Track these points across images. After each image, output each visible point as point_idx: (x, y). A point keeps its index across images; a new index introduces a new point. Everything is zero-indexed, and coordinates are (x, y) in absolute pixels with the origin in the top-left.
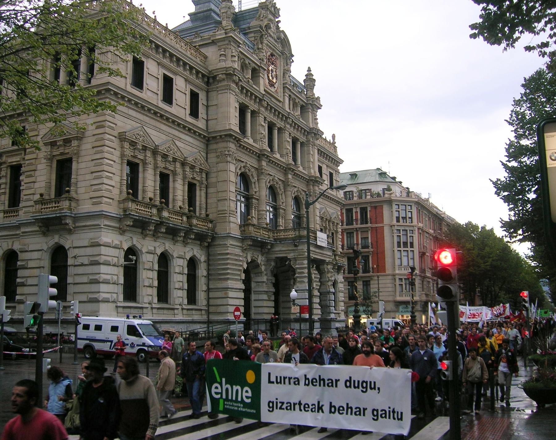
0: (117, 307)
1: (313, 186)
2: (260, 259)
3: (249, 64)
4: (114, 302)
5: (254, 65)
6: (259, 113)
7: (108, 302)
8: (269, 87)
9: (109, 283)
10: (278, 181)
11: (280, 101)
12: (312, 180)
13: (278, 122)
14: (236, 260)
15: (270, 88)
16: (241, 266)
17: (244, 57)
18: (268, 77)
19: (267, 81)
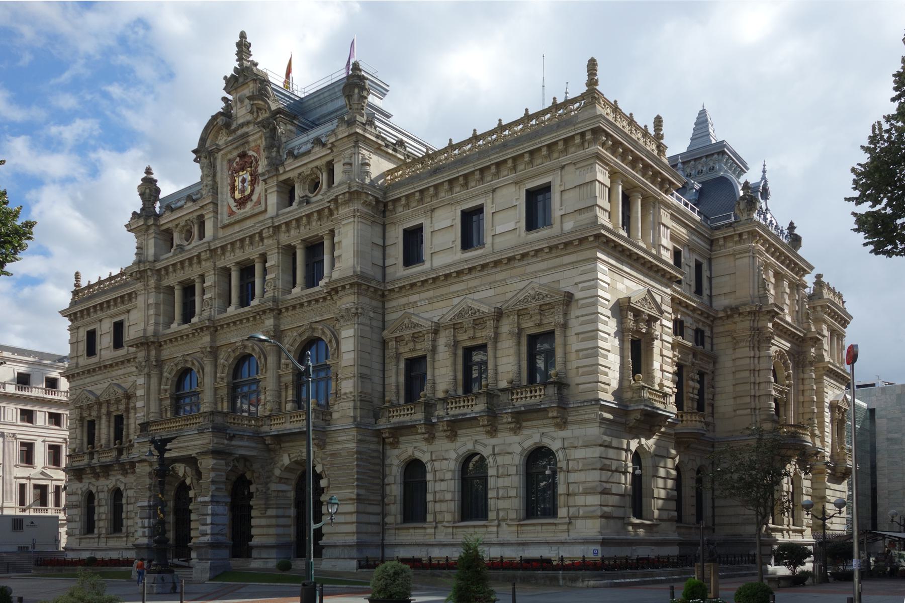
10: (247, 343)
15: (242, 211)
18: (234, 198)
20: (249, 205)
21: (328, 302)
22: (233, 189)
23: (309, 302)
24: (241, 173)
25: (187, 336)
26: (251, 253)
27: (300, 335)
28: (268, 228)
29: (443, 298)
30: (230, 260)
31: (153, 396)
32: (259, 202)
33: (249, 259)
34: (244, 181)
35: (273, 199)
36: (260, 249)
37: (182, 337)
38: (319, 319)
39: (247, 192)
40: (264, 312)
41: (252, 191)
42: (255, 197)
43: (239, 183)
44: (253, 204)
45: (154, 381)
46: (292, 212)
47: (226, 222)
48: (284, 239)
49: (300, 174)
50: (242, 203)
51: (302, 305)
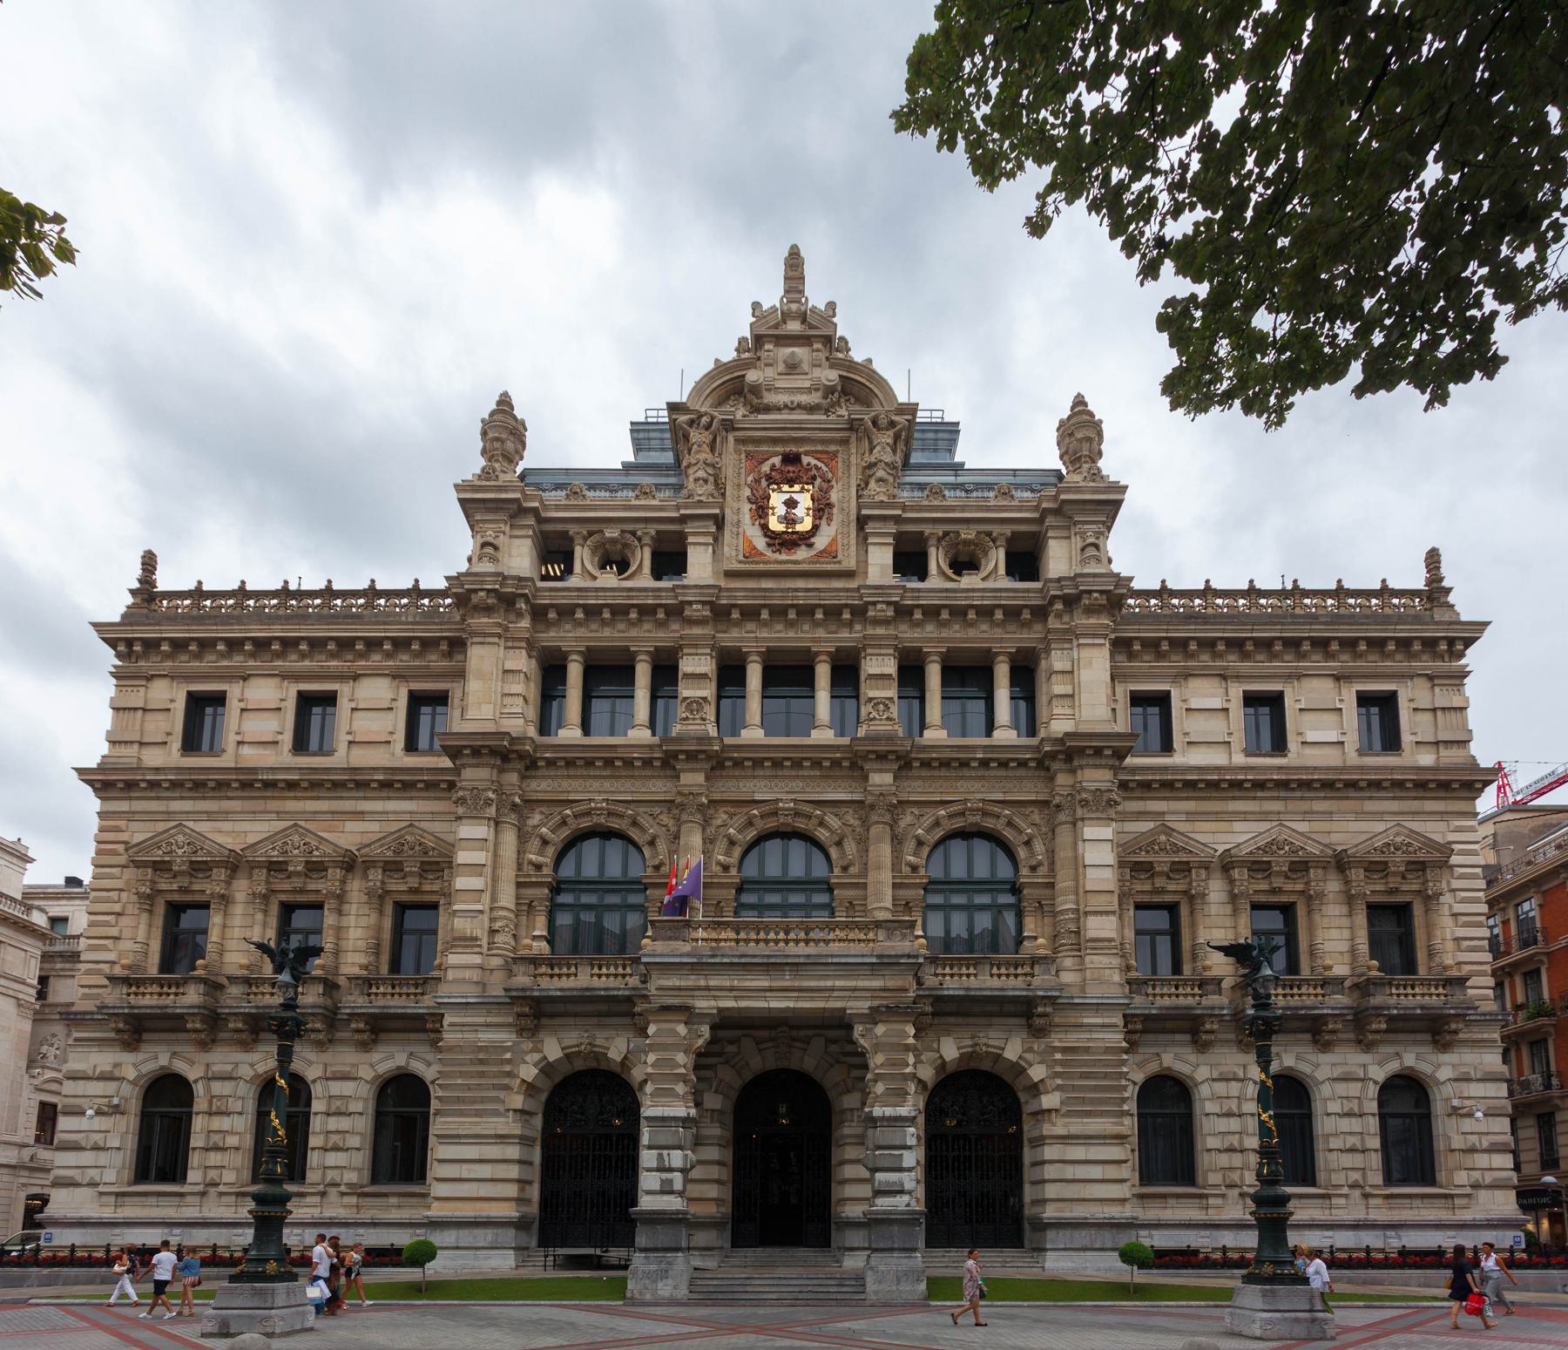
0: (101, 1194)
1: (1073, 771)
2: (616, 1047)
3: (634, 533)
4: (93, 1184)
5: (652, 529)
6: (681, 647)
7: (73, 1184)
8: (769, 553)
9: (83, 1149)
10: (807, 808)
11: (850, 574)
12: (1052, 756)
13: (814, 640)
14: (482, 1062)
15: (783, 557)
16: (509, 1074)
17: (594, 527)
18: (765, 527)
19: (760, 543)
20: (802, 554)
21: (1022, 772)
22: (761, 510)
23: (984, 763)
24: (786, 488)
25: (629, 763)
26: (822, 639)
27: (951, 816)
28: (889, 603)
29: (1217, 817)
30: (752, 639)
31: (508, 874)
32: (829, 553)
33: (808, 650)
34: (791, 504)
35: (880, 560)
36: (847, 637)
37: (609, 762)
38: (1000, 797)
39: (799, 528)
40: (881, 757)
41: (815, 528)
42: (821, 542)
43: (777, 500)
44: (813, 553)
45: (509, 838)
46: (919, 590)
47: (736, 566)
48: (909, 635)
49: (946, 534)
50: (786, 541)
51: (964, 764)
